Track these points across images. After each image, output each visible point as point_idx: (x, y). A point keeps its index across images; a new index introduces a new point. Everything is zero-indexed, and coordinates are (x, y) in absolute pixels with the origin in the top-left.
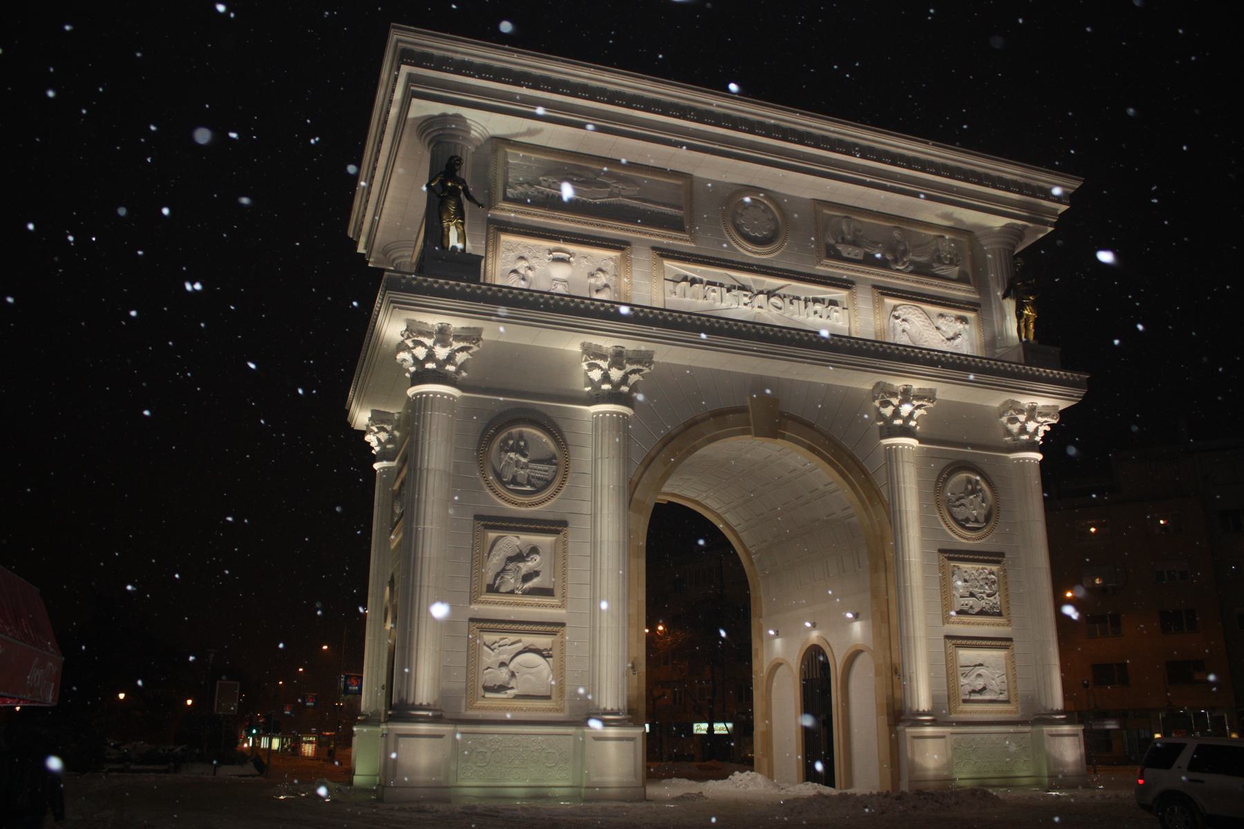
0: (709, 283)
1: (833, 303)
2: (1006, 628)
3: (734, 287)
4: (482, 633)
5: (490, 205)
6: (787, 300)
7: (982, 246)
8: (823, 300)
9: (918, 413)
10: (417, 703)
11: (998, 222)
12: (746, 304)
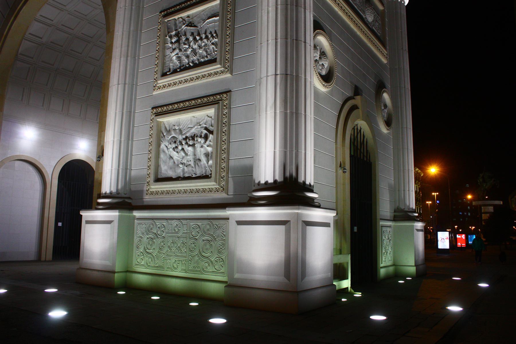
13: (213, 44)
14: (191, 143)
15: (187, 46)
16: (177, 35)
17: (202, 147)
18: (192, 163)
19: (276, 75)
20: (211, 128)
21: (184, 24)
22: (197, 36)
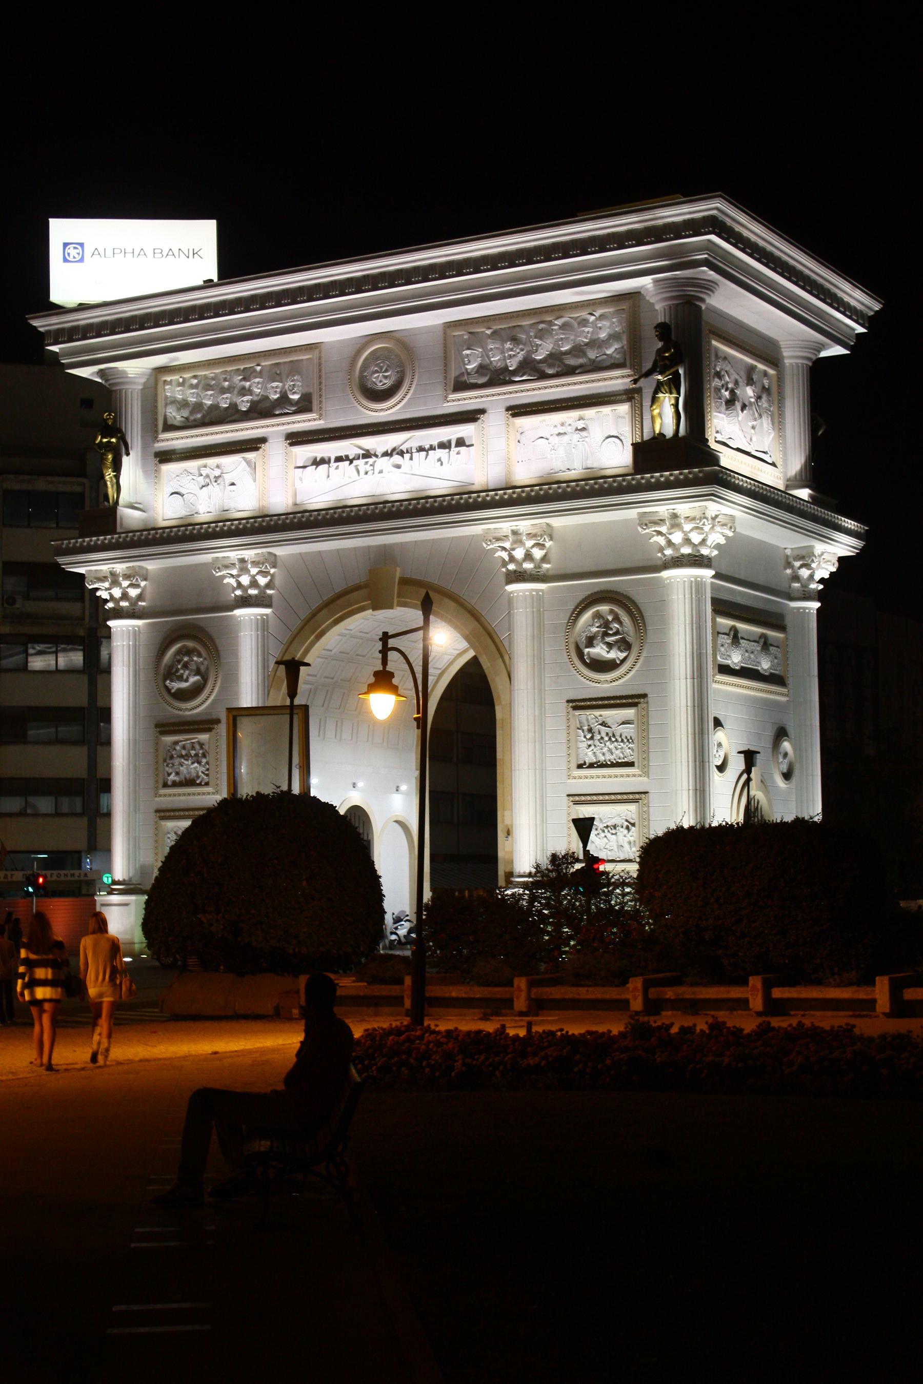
0: (339, 459)
1: (461, 443)
2: (640, 778)
3: (358, 458)
4: (161, 821)
5: (155, 439)
6: (407, 456)
7: (653, 304)
8: (449, 442)
9: (538, 554)
10: (116, 879)
11: (646, 282)
12: (366, 473)
13: (629, 748)
14: (614, 832)
15: (603, 745)
16: (590, 730)
17: (625, 836)
18: (615, 848)
19: (689, 790)
20: (632, 821)
21: (597, 722)
22: (612, 737)
